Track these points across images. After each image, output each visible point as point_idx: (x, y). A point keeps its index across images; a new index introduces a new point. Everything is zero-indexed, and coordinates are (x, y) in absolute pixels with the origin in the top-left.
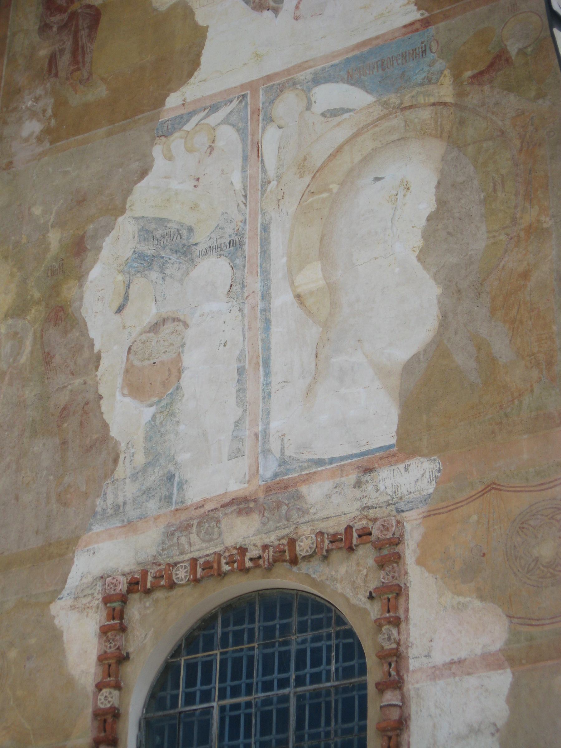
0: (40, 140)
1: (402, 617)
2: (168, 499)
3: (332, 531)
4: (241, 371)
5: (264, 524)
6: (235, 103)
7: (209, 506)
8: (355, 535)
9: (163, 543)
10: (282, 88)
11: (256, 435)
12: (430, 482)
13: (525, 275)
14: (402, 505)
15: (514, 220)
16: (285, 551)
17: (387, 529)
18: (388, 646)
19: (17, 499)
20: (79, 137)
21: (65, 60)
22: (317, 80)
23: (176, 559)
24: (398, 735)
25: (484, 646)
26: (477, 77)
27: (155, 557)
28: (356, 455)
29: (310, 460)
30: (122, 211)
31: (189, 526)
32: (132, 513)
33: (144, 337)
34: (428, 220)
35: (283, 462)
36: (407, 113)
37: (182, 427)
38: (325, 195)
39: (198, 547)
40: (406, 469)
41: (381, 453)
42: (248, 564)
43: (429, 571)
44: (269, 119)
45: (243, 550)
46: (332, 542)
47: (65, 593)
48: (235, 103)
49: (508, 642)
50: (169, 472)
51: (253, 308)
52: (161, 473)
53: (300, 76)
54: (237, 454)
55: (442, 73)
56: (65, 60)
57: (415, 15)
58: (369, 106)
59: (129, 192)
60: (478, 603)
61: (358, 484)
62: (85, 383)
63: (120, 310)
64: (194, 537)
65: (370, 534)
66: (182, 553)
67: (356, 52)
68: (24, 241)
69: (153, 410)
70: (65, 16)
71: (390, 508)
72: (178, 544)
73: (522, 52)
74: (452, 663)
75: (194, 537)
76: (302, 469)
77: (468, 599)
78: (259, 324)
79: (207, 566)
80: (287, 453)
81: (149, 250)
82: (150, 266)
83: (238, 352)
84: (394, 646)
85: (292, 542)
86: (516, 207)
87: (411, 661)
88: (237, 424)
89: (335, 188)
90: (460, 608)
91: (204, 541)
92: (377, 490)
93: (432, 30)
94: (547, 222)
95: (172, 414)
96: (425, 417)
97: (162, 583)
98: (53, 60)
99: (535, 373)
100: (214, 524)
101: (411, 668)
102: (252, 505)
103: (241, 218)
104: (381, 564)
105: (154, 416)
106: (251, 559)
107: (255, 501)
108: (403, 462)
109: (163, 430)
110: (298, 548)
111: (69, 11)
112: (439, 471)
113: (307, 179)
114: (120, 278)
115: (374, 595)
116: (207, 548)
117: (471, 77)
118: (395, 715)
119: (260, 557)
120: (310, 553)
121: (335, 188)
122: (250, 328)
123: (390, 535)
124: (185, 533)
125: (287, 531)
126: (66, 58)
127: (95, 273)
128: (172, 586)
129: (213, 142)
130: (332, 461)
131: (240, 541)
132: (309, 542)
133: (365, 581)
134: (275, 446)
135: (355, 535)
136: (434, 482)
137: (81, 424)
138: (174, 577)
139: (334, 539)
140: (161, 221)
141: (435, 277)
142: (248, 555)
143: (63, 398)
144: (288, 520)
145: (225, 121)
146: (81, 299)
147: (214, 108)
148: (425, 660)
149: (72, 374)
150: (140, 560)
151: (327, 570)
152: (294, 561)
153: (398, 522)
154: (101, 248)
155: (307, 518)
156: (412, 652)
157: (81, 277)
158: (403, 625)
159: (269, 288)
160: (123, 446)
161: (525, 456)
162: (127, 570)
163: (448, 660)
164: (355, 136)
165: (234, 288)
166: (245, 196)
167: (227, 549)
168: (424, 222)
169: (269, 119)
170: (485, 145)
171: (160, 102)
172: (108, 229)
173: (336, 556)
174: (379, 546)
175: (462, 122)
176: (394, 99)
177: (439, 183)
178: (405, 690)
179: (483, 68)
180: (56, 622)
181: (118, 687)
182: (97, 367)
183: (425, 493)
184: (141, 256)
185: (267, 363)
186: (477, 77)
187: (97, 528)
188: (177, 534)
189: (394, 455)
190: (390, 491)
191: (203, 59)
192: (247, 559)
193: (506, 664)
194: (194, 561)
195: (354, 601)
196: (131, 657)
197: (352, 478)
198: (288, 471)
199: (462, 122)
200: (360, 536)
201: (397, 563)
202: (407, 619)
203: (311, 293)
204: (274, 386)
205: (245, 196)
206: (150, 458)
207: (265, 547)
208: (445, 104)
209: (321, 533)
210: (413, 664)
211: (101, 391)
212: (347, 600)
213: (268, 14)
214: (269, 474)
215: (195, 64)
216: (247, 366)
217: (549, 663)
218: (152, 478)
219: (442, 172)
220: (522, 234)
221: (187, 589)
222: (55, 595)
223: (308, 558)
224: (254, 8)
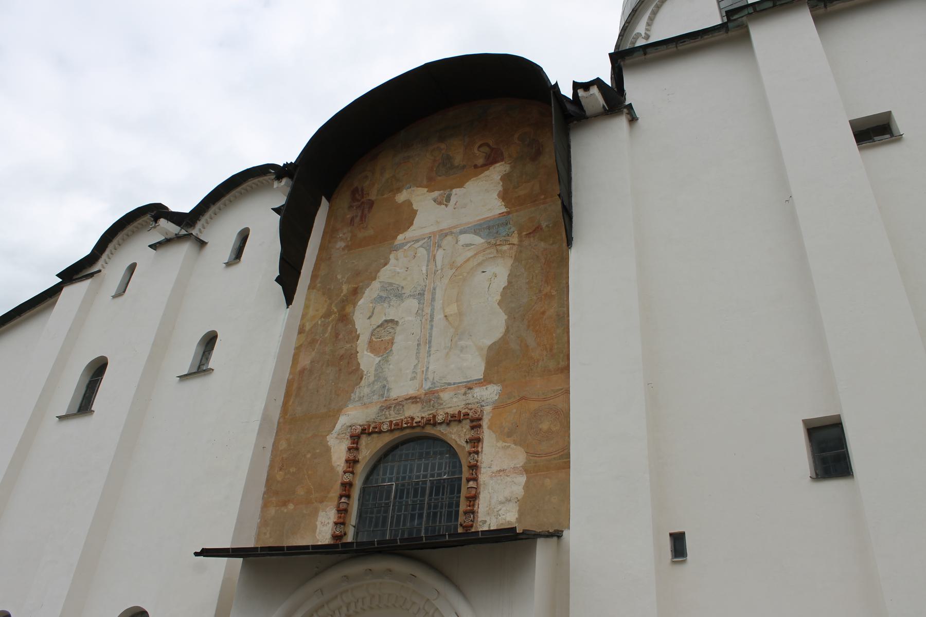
0: (343, 249)
1: (480, 450)
2: (382, 395)
3: (452, 413)
4: (419, 345)
5: (423, 408)
6: (426, 239)
7: (399, 400)
8: (462, 415)
9: (378, 414)
10: (446, 235)
11: (423, 371)
12: (496, 395)
13: (543, 313)
14: (483, 403)
15: (540, 291)
16: (431, 420)
17: (476, 413)
18: (473, 462)
19: (317, 391)
20: (360, 249)
21: (357, 220)
23: (383, 420)
24: (474, 501)
25: (515, 464)
26: (528, 235)
27: (374, 419)
28: (465, 382)
29: (445, 383)
30: (375, 279)
31: (390, 407)
32: (366, 400)
33: (378, 330)
34: (503, 289)
35: (433, 383)
36: (498, 247)
37: (391, 366)
38: (461, 277)
39: (393, 416)
40: (486, 389)
41: (477, 382)
42: (415, 424)
43: (493, 432)
44: (439, 246)
45: (413, 419)
46: (452, 417)
47: (334, 432)
48: (426, 239)
49: (526, 463)
50: (384, 385)
51: (426, 320)
52: (380, 384)
53: (454, 231)
54: (413, 379)
55: (514, 232)
56: (357, 220)
57: (504, 210)
58: (482, 243)
59: (378, 271)
60: (513, 446)
61: (465, 394)
62: (352, 346)
63: (369, 318)
64: (392, 412)
65: (469, 415)
66: (386, 418)
67: (478, 223)
68: (332, 288)
69: (380, 359)
70: (359, 203)
71: (478, 404)
72: (385, 415)
73: (547, 226)
74: (500, 471)
75: (392, 412)
76: (441, 386)
77: (509, 444)
78: (429, 327)
79: (397, 424)
80: (435, 380)
81: (384, 294)
82: (384, 301)
83: (418, 337)
84: (476, 462)
85: (434, 417)
86: (541, 286)
87: (482, 469)
88: (415, 366)
89: (465, 274)
90: (505, 448)
91: (396, 414)
92: (473, 397)
93: (510, 216)
94: (554, 293)
95: (387, 361)
96: (496, 368)
97: (376, 430)
98: (352, 220)
99: (545, 353)
100: (401, 407)
101: (482, 472)
102: (418, 400)
103: (424, 284)
104: (472, 428)
105: (380, 361)
106: (416, 423)
107: (420, 398)
108: (485, 386)
109: (383, 367)
110: (437, 419)
111: (361, 201)
112: (501, 390)
113: (454, 270)
114: (371, 305)
115: (468, 440)
116: (397, 417)
117: (526, 235)
118: (473, 492)
119: (420, 422)
120: (442, 421)
121: (465, 274)
122: (424, 328)
123: (477, 416)
124: (388, 410)
125: (433, 412)
126: (358, 218)
127: (360, 303)
128: (380, 432)
129: (416, 254)
130: (454, 384)
131: (412, 415)
132: (441, 417)
133: (465, 435)
134: (430, 376)
135: (462, 415)
136: (498, 395)
137: (348, 363)
138: (382, 428)
139: (453, 416)
140: (391, 284)
141: (504, 312)
142: (415, 421)
143: (342, 352)
144: (433, 407)
145: (421, 246)
146: (354, 313)
147: (417, 241)
148: (489, 469)
149: (347, 342)
150: (368, 420)
151: (448, 429)
152: (435, 424)
153: (481, 411)
154: (364, 293)
155: (442, 407)
156: (483, 466)
157: (355, 304)
158: (480, 454)
159: (433, 312)
160: (365, 373)
161: (538, 386)
162: (362, 424)
163: (498, 469)
164: (476, 254)
165: (419, 311)
166: (427, 276)
167: (406, 418)
168: (501, 289)
170: (529, 261)
171: (395, 238)
173: (452, 424)
174: (472, 421)
175: (521, 252)
176: (493, 241)
177: (509, 275)
178: (479, 481)
179: (531, 231)
180: (329, 443)
181: (352, 473)
182: (357, 340)
183: (494, 399)
184: (381, 297)
185: (430, 342)
186: (528, 235)
187: (350, 406)
188: (385, 410)
189: (482, 383)
190: (479, 398)
191: (414, 222)
192: (414, 422)
193: (524, 473)
194: (391, 422)
195: (459, 442)
196: (360, 460)
197: (463, 391)
198: (435, 387)
199: (521, 252)
200: (464, 415)
201: (479, 428)
202: (482, 451)
203: (451, 315)
204: (432, 352)
205: (427, 276)
206: (376, 378)
207: (422, 418)
208: (514, 244)
209: (447, 413)
210: (483, 470)
211: (358, 350)
212: (456, 442)
213: (443, 206)
214: (427, 388)
215: (412, 224)
216: (421, 343)
217: (543, 473)
218: (376, 386)
219: (511, 270)
220: (543, 297)
221: (387, 434)
222: (330, 431)
223: (440, 424)
224: (438, 204)
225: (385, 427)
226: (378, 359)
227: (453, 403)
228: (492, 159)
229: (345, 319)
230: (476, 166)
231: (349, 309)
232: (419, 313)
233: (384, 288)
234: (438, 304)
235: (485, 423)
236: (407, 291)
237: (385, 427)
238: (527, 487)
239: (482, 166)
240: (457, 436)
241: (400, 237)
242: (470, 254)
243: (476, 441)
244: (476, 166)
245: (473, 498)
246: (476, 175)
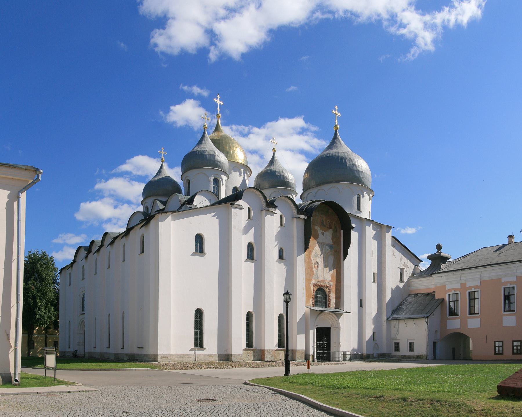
10: (324, 244)
22: (326, 245)
127: (312, 255)
169: (323, 247)
227: (327, 284)
228: (330, 228)
229: (310, 258)
231: (310, 255)
239: (329, 228)
240: (327, 290)
243: (329, 292)
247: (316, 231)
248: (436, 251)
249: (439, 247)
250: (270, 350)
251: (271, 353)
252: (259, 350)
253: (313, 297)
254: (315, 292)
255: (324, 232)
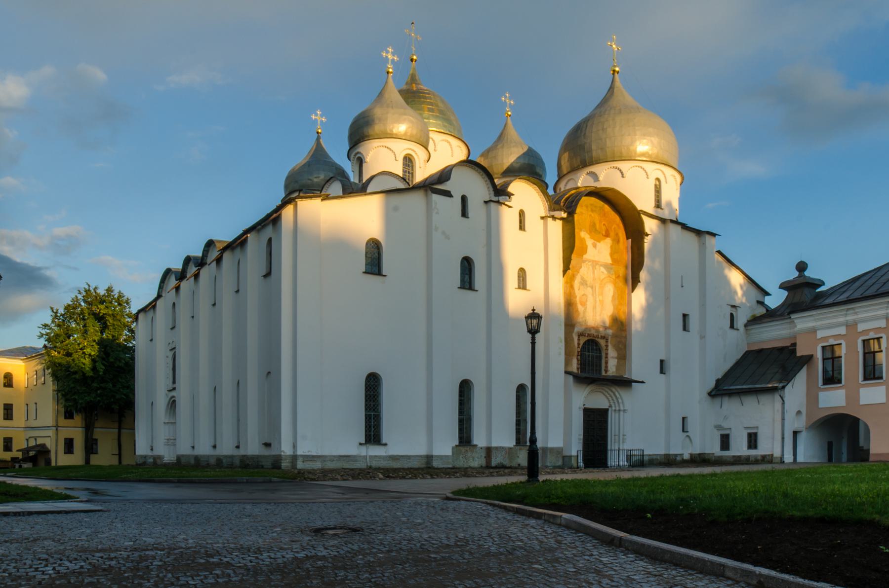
22: (601, 265)
81: (582, 282)
147: (589, 262)
152: (598, 338)
157: (574, 281)
171: (582, 256)
172: (577, 275)
215: (586, 252)
222: (573, 332)
225: (587, 335)
226: (583, 309)
228: (607, 235)
229: (572, 287)
230: (603, 234)
232: (593, 295)
233: (582, 278)
234: (597, 293)
235: (609, 341)
236: (588, 283)
237: (587, 335)
238: (618, 361)
239: (605, 236)
240: (602, 342)
241: (585, 256)
242: (603, 277)
243: (607, 346)
244: (603, 234)
245: (607, 363)
246: (604, 239)
247: (583, 241)
248: (796, 274)
249: (802, 267)
250: (500, 447)
251: (503, 453)
252: (481, 448)
253: (578, 356)
254: (581, 346)
255: (598, 243)
